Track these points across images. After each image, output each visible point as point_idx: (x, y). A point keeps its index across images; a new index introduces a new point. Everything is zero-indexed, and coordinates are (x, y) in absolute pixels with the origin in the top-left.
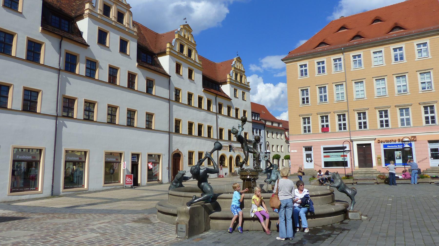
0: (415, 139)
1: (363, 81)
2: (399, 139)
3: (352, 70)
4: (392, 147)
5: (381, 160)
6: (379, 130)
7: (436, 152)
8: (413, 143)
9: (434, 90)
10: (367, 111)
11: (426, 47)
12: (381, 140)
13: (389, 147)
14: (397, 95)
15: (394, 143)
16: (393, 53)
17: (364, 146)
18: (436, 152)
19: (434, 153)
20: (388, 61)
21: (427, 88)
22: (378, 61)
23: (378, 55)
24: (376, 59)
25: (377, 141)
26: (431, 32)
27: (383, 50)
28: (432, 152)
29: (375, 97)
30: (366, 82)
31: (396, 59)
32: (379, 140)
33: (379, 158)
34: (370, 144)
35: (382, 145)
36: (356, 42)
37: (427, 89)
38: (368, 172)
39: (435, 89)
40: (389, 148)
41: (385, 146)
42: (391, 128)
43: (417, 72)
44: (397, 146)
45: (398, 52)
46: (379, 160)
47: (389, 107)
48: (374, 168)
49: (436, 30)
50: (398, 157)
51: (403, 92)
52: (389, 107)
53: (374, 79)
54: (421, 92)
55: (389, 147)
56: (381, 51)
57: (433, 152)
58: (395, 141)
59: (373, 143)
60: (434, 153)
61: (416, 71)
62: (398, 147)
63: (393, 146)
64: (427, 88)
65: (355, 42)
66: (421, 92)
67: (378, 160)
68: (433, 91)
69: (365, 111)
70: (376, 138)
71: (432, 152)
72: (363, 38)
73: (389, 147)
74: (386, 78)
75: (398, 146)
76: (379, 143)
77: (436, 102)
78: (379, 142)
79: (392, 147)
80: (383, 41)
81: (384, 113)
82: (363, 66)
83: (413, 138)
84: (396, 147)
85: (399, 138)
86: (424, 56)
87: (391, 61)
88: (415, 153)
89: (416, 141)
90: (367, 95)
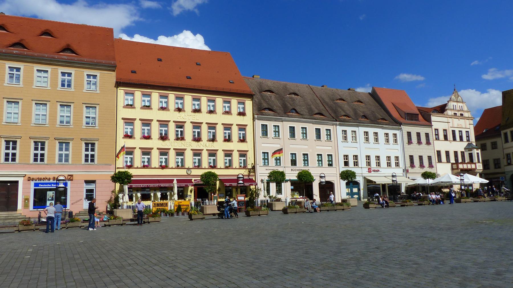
0: (72, 178)
1: (19, 102)
2: (54, 177)
3: (5, 85)
4: (44, 187)
5: (28, 201)
6: (31, 164)
7: (91, 193)
8: (69, 183)
9: (97, 127)
10: (18, 141)
11: (95, 80)
12: (32, 177)
13: (41, 187)
14: (59, 126)
15: (48, 181)
16: (60, 77)
17: (9, 184)
18: (91, 193)
19: (90, 194)
20: (54, 84)
21: (90, 124)
22: (42, 82)
23: (43, 74)
24: (39, 79)
25: (26, 178)
26: (102, 65)
27: (49, 70)
28: (87, 193)
29: (31, 124)
30: (22, 104)
31: (63, 85)
32: (29, 178)
33: (26, 200)
34: (17, 182)
35: (32, 183)
36: (17, 52)
37: (90, 125)
38: (9, 218)
39: (99, 126)
40: (41, 187)
41: (36, 185)
42: (47, 164)
43: (84, 104)
44: (50, 185)
45: (66, 77)
46: (27, 201)
47: (47, 139)
48: (18, 212)
49: (107, 65)
50: (50, 199)
51: (66, 123)
52: (47, 139)
53: (34, 102)
54: (85, 127)
55: (42, 186)
56: (47, 71)
57: (89, 193)
58: (49, 179)
59: (21, 180)
60: (90, 194)
61: (83, 103)
62: (51, 186)
63: (46, 186)
64: (90, 124)
65: (15, 51)
66: (85, 127)
67: (25, 202)
68: (96, 128)
69: (17, 140)
70: (26, 175)
71: (87, 193)
72: (27, 49)
73: (41, 187)
74: (48, 103)
75: (52, 185)
76: (29, 180)
77: (97, 140)
78: (30, 179)
79: (44, 187)
80: (51, 60)
81: (39, 145)
82: (21, 83)
83: (69, 177)
84: (49, 187)
85: (54, 176)
86: (92, 89)
87: (58, 85)
88: (69, 194)
89: (72, 180)
90: (21, 120)
